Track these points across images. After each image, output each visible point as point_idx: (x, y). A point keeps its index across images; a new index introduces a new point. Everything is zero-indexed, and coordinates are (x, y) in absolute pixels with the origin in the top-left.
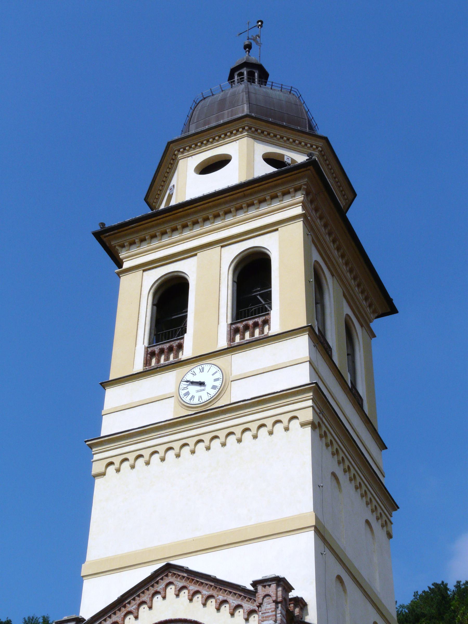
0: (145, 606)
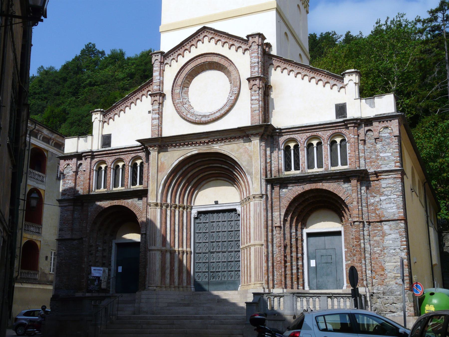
0: (194, 47)
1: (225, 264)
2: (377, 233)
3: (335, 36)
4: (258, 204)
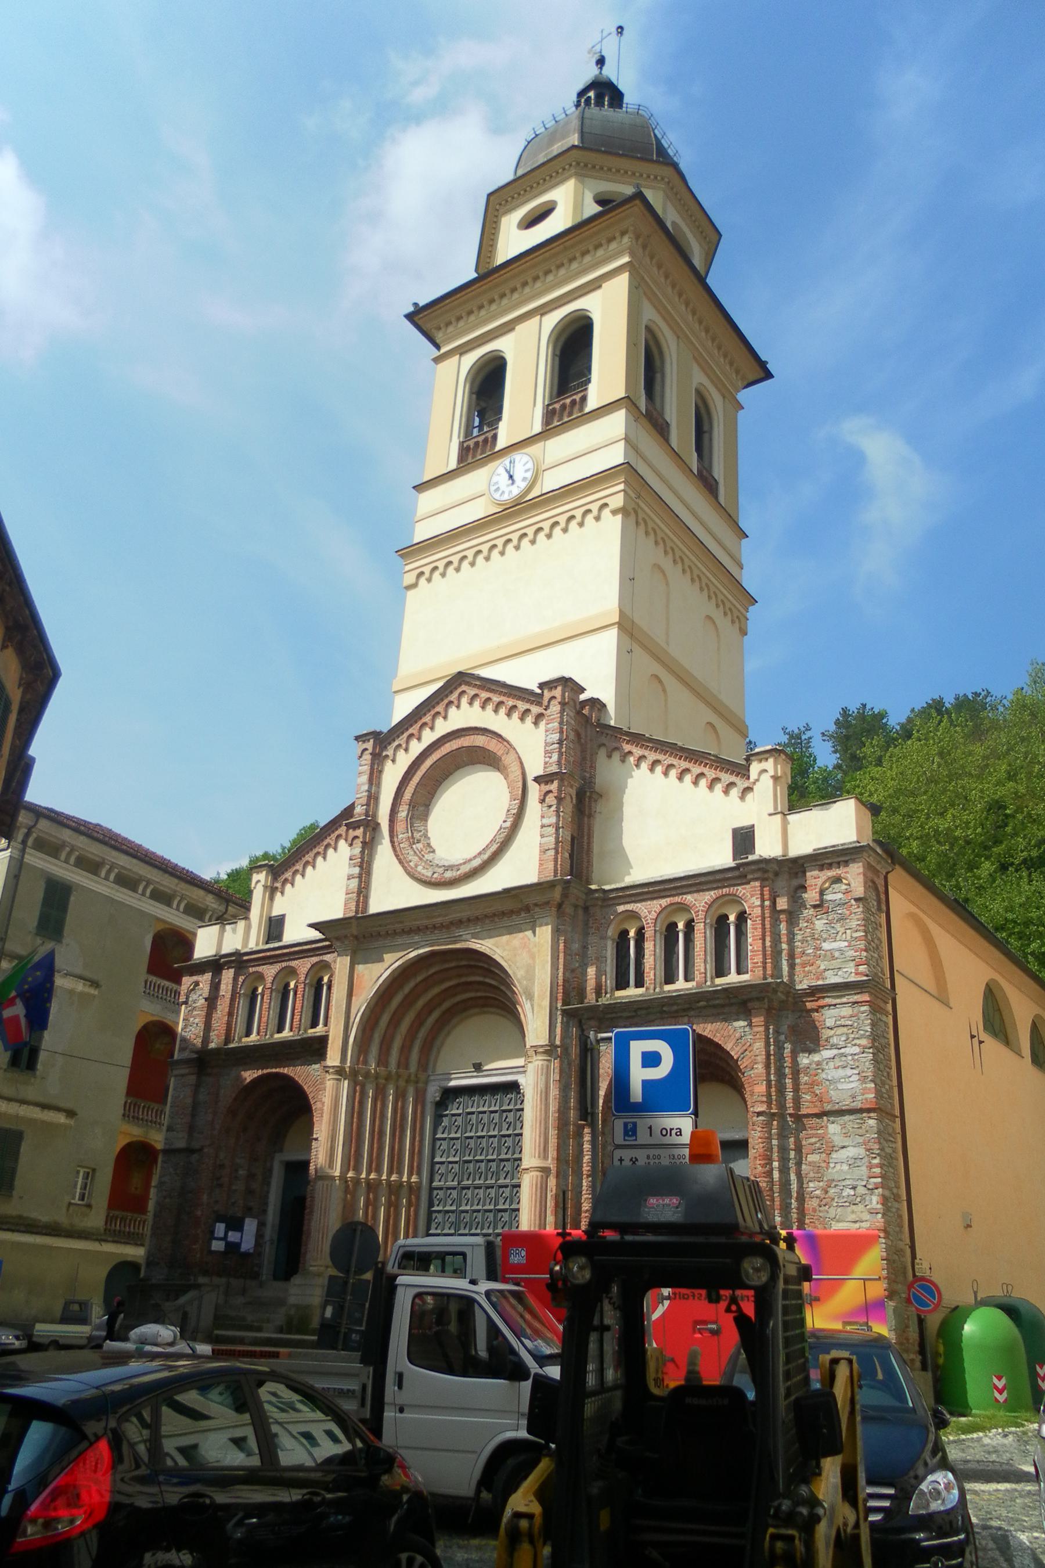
1: (491, 1215)
3: (989, 699)
4: (542, 1069)
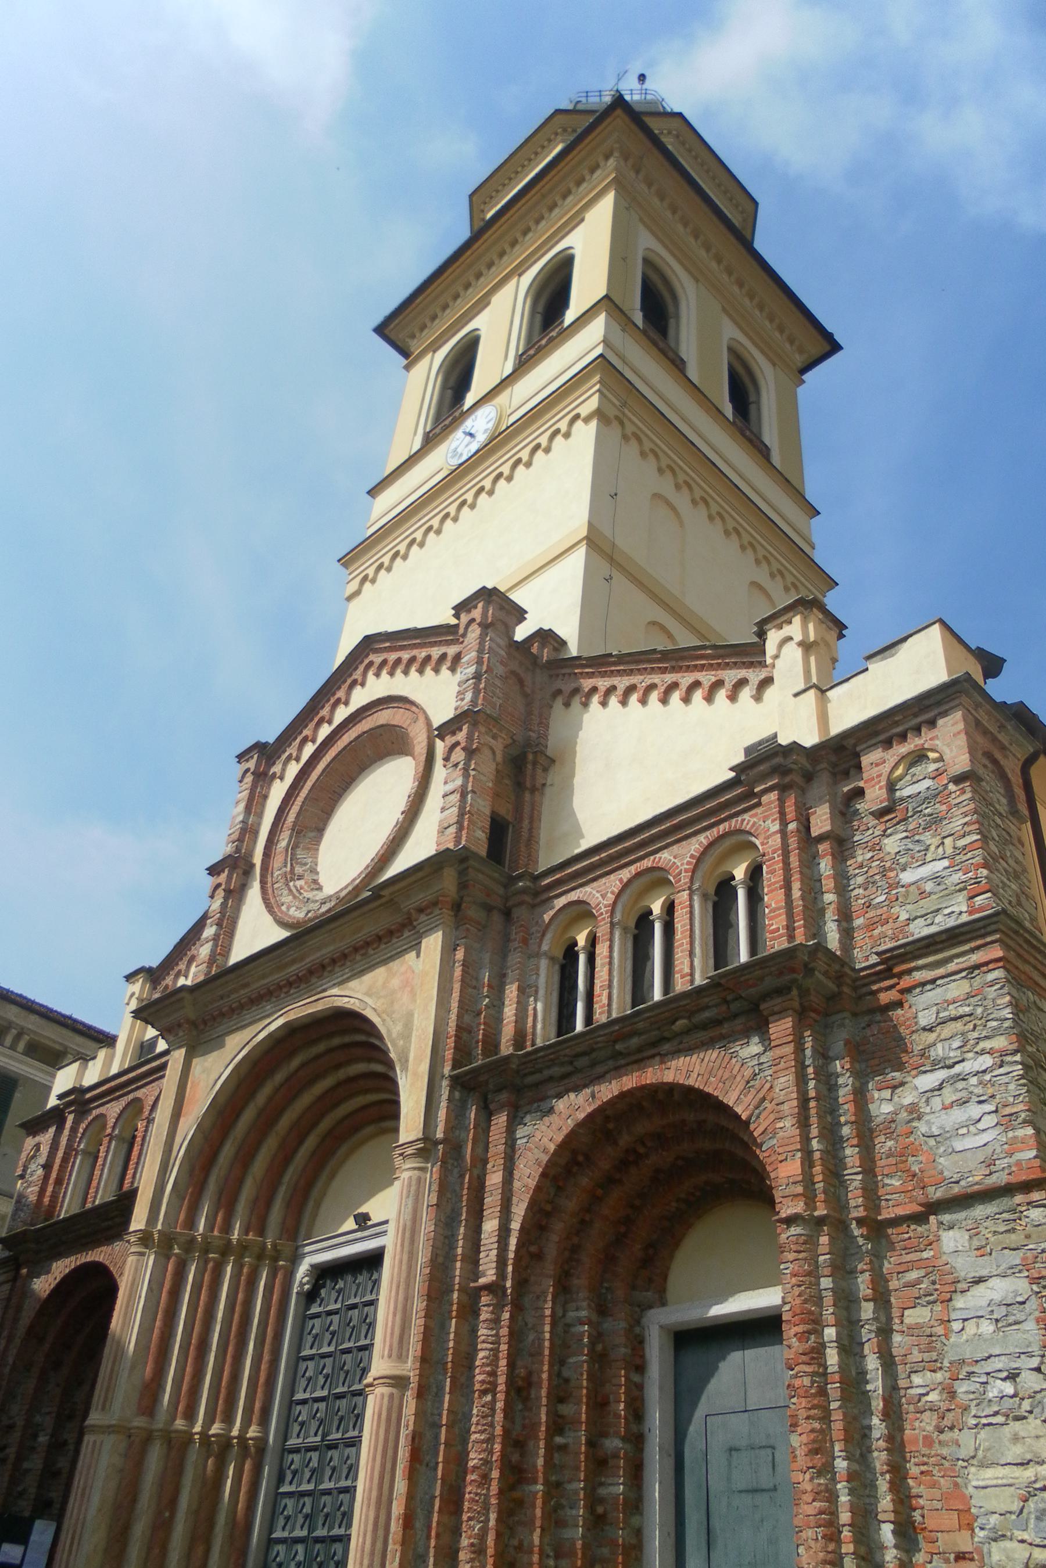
2: (919, 1281)
